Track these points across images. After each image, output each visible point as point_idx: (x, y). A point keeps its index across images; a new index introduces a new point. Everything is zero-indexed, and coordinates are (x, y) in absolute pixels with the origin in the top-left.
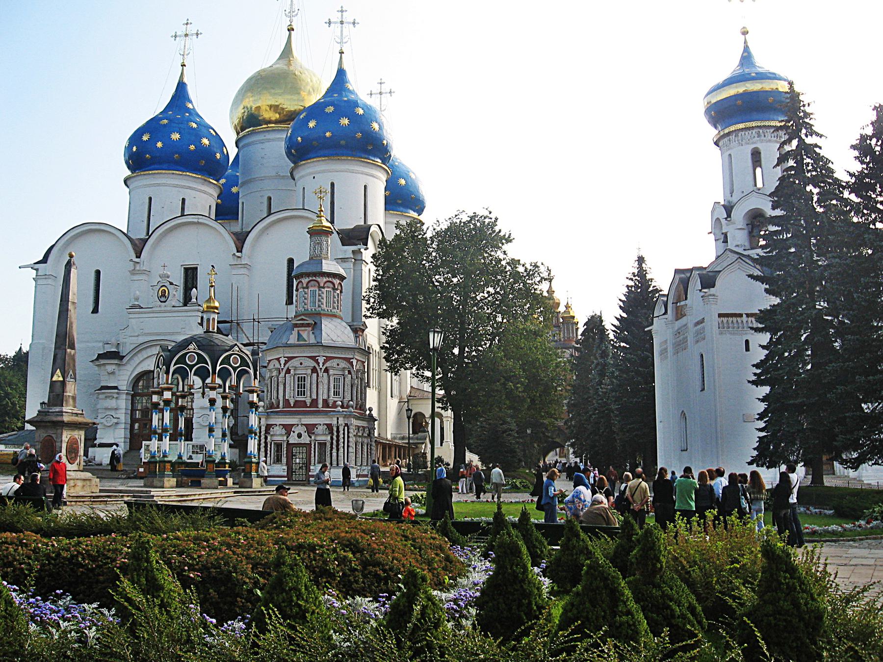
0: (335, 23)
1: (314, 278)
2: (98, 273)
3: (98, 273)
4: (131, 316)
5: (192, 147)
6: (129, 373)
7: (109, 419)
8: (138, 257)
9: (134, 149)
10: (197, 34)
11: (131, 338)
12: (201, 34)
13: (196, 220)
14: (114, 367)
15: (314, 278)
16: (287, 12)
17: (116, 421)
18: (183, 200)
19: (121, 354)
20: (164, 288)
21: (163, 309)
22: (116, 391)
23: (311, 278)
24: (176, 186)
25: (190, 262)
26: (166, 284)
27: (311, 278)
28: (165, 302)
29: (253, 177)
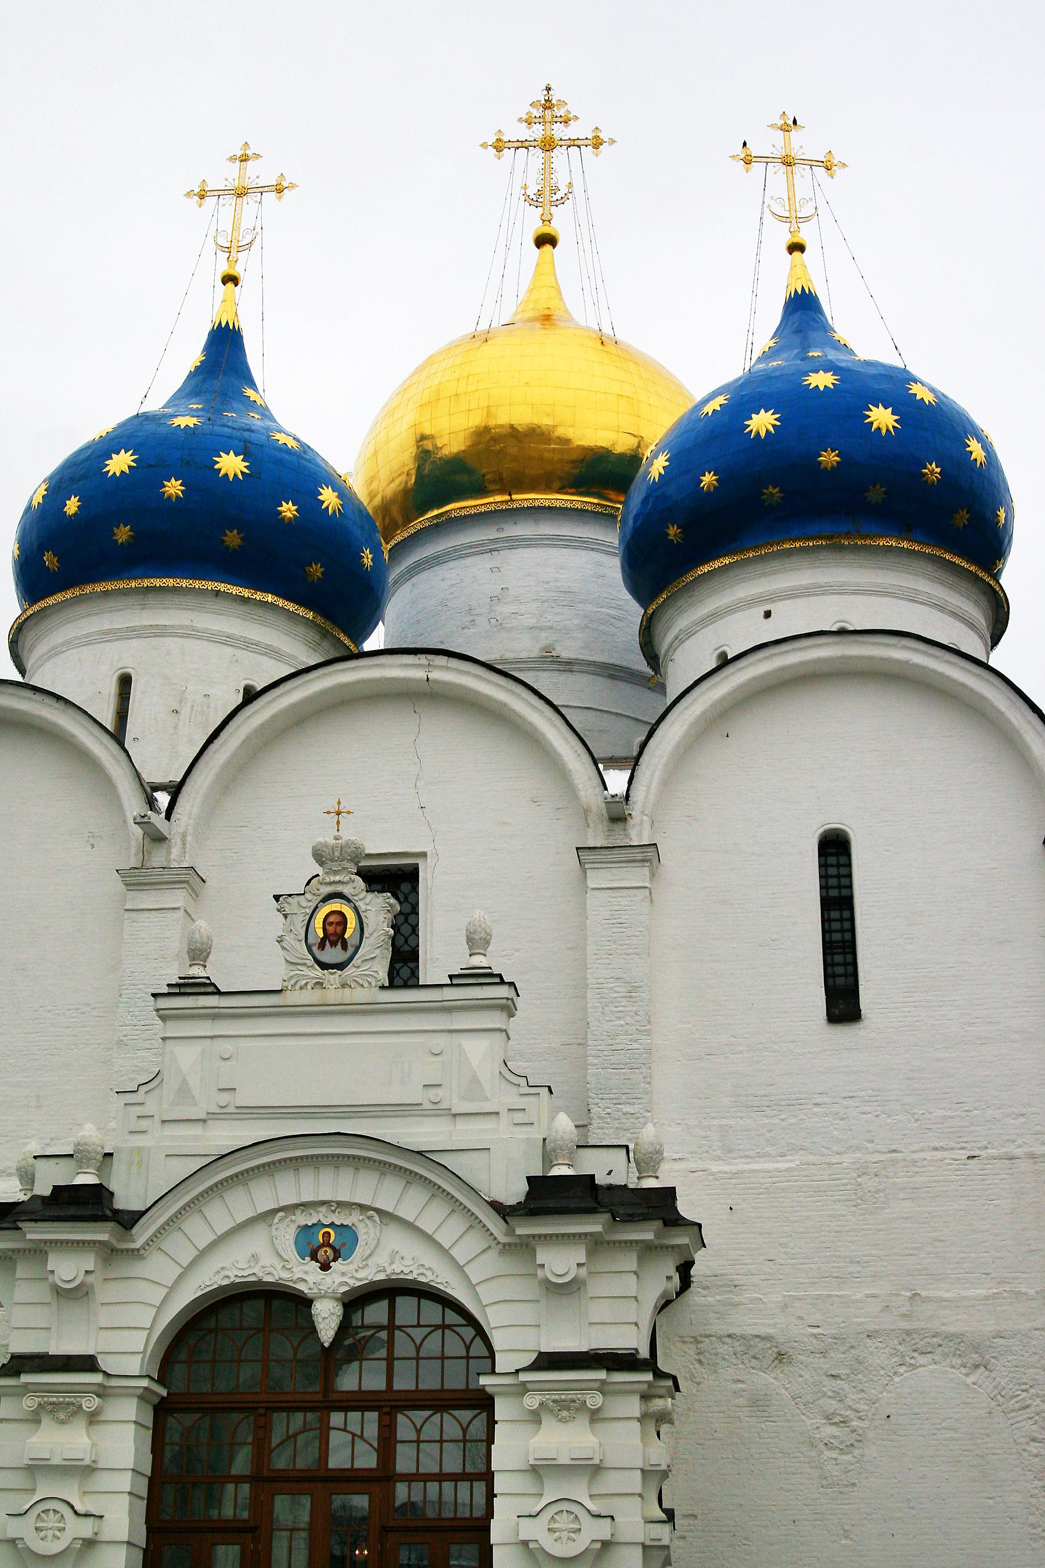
0: (767, 160)
4: (175, 1029)
5: (288, 510)
6: (157, 1295)
7: (51, 1521)
9: (72, 506)
10: (279, 190)
11: (171, 1131)
12: (292, 186)
13: (420, 674)
14: (89, 1261)
16: (532, 191)
17: (85, 1529)
19: (119, 1204)
20: (335, 905)
21: (333, 995)
22: (96, 1378)
24: (229, 640)
26: (346, 890)
28: (341, 966)
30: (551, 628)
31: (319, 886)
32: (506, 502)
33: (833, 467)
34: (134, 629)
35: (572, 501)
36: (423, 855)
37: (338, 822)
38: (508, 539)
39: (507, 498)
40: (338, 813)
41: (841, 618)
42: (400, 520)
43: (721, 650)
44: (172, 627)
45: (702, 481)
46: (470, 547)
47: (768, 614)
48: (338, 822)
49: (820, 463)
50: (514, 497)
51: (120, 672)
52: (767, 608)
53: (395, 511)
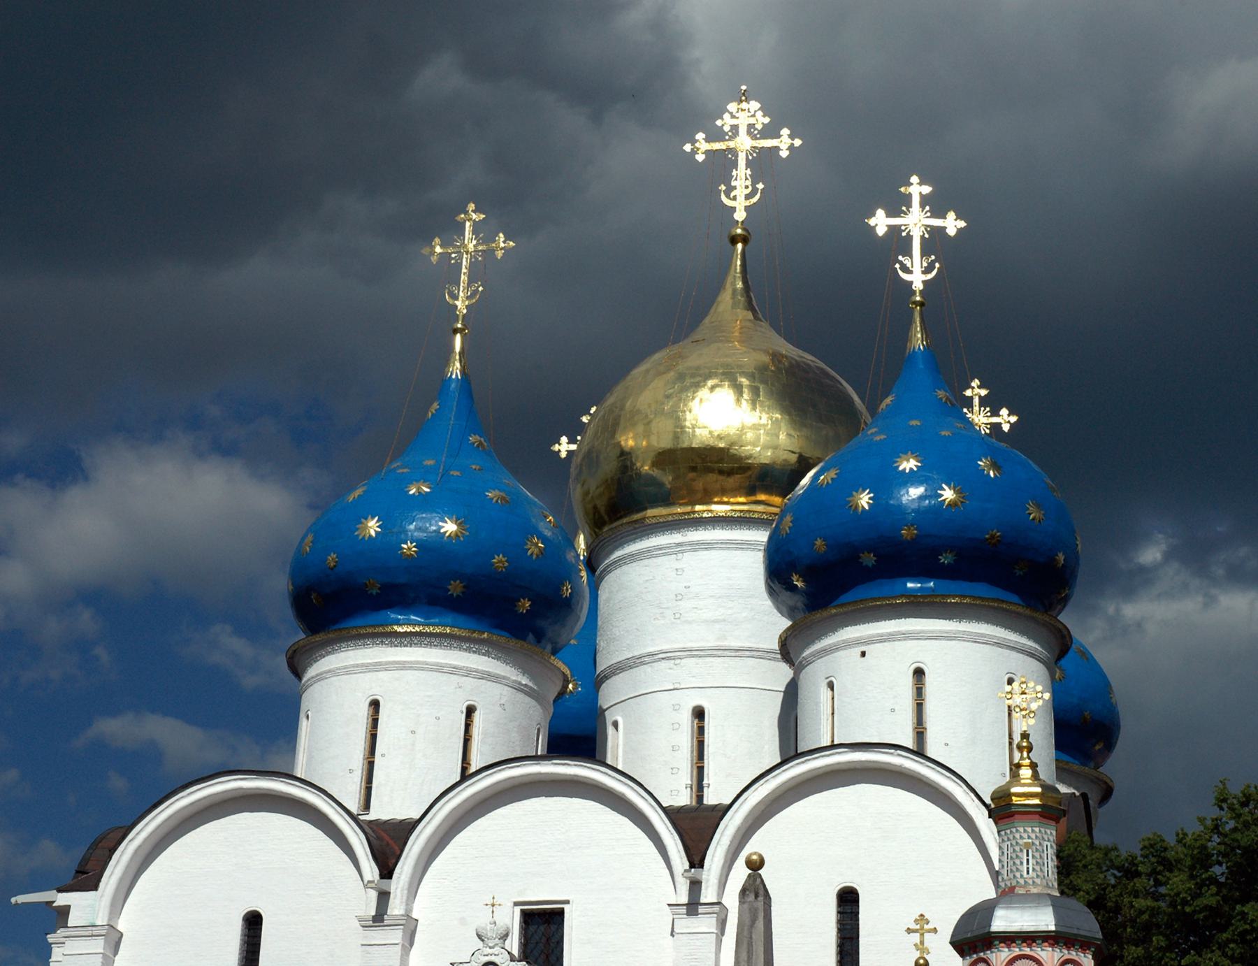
1: (1027, 951)
2: (253, 922)
3: (253, 922)
8: (387, 872)
15: (1027, 951)
18: (470, 711)
23: (1016, 951)
24: (455, 670)
25: (541, 893)
27: (1016, 951)
29: (651, 649)
30: (724, 620)
31: (480, 957)
32: (688, 513)
33: (912, 539)
34: (380, 664)
35: (741, 511)
36: (567, 902)
37: (493, 912)
38: (690, 544)
39: (689, 509)
40: (493, 905)
41: (919, 659)
42: (606, 518)
43: (830, 679)
44: (408, 662)
45: (816, 544)
46: (660, 549)
47: (863, 654)
48: (493, 912)
49: (902, 535)
50: (698, 508)
51: (372, 698)
52: (863, 648)
53: (602, 510)
